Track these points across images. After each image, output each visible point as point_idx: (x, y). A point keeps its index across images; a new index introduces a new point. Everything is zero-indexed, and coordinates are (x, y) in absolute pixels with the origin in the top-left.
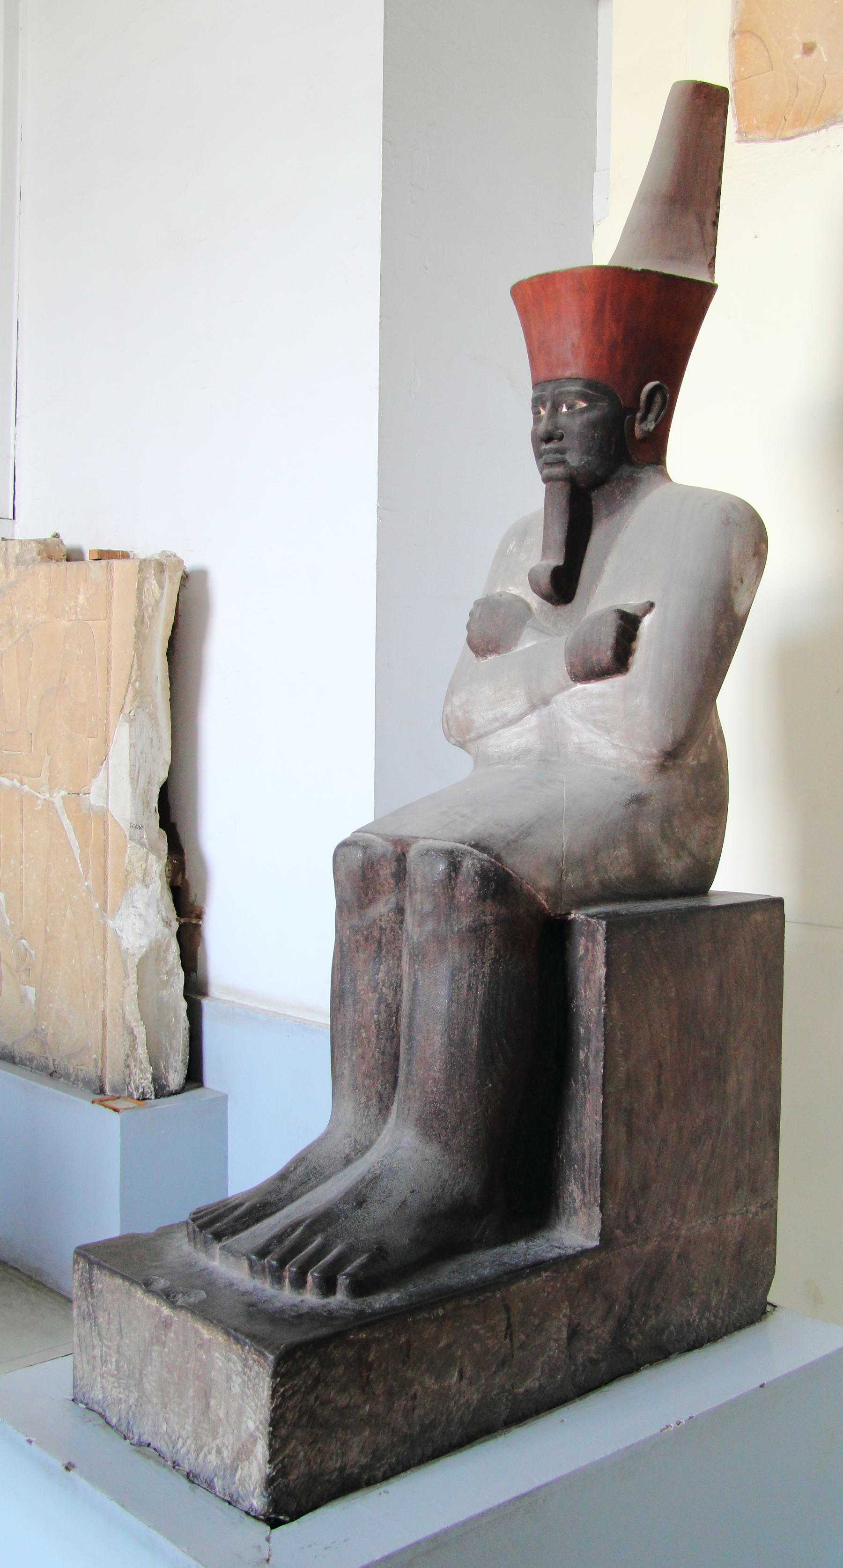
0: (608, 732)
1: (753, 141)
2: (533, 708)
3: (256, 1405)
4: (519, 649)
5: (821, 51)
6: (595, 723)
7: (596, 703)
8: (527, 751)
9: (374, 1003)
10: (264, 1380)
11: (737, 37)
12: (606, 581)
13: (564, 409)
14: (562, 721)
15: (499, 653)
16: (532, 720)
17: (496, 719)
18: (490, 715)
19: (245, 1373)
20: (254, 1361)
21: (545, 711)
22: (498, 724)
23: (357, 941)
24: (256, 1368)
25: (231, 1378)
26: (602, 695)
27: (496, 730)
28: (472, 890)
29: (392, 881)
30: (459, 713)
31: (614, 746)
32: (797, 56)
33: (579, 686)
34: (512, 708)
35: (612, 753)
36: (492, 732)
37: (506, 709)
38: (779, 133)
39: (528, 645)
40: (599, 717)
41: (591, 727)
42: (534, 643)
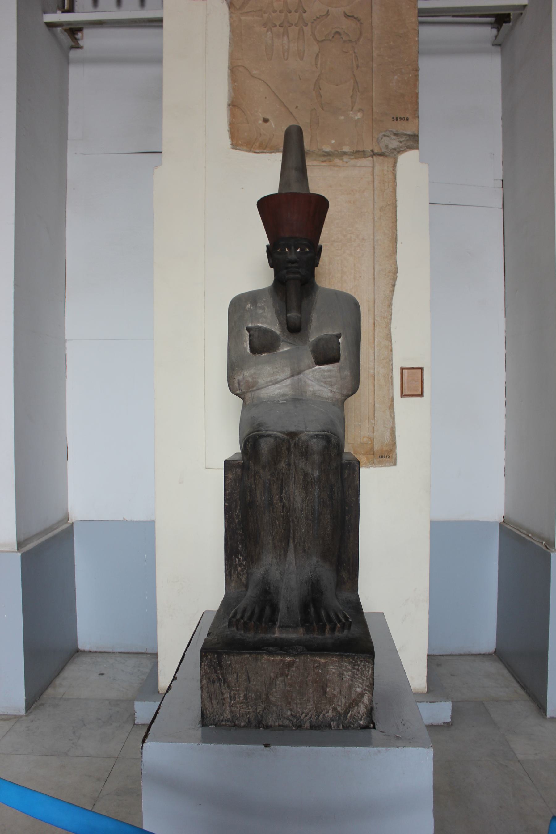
0: (332, 385)
1: (239, 150)
2: (292, 376)
3: (363, 680)
4: (281, 351)
5: (272, 122)
6: (325, 383)
7: (327, 374)
8: (284, 395)
9: (281, 508)
10: (369, 667)
11: (231, 107)
12: (314, 324)
13: (298, 251)
14: (305, 382)
15: (270, 353)
16: (289, 382)
17: (271, 381)
18: (269, 379)
19: (354, 669)
20: (361, 661)
21: (296, 378)
22: (271, 384)
23: (273, 480)
24: (363, 664)
25: (343, 674)
26: (329, 371)
27: (268, 386)
28: (336, 451)
29: (287, 452)
30: (250, 379)
31: (331, 391)
32: (261, 122)
33: (317, 367)
34: (279, 377)
35: (330, 394)
36: (265, 387)
37: (278, 377)
38: (252, 149)
39: (286, 349)
40: (329, 380)
41: (322, 384)
42: (288, 348)
